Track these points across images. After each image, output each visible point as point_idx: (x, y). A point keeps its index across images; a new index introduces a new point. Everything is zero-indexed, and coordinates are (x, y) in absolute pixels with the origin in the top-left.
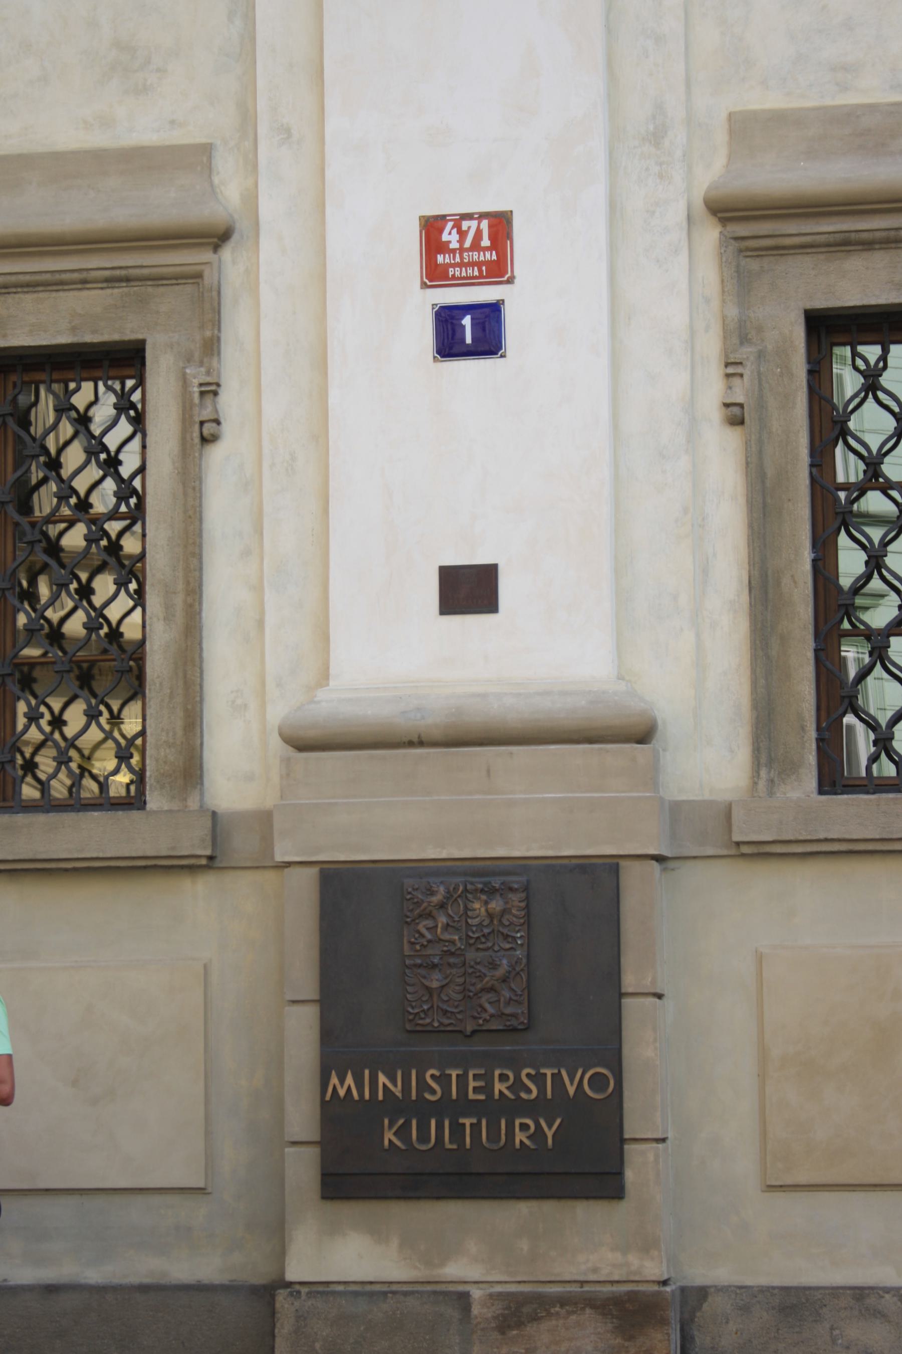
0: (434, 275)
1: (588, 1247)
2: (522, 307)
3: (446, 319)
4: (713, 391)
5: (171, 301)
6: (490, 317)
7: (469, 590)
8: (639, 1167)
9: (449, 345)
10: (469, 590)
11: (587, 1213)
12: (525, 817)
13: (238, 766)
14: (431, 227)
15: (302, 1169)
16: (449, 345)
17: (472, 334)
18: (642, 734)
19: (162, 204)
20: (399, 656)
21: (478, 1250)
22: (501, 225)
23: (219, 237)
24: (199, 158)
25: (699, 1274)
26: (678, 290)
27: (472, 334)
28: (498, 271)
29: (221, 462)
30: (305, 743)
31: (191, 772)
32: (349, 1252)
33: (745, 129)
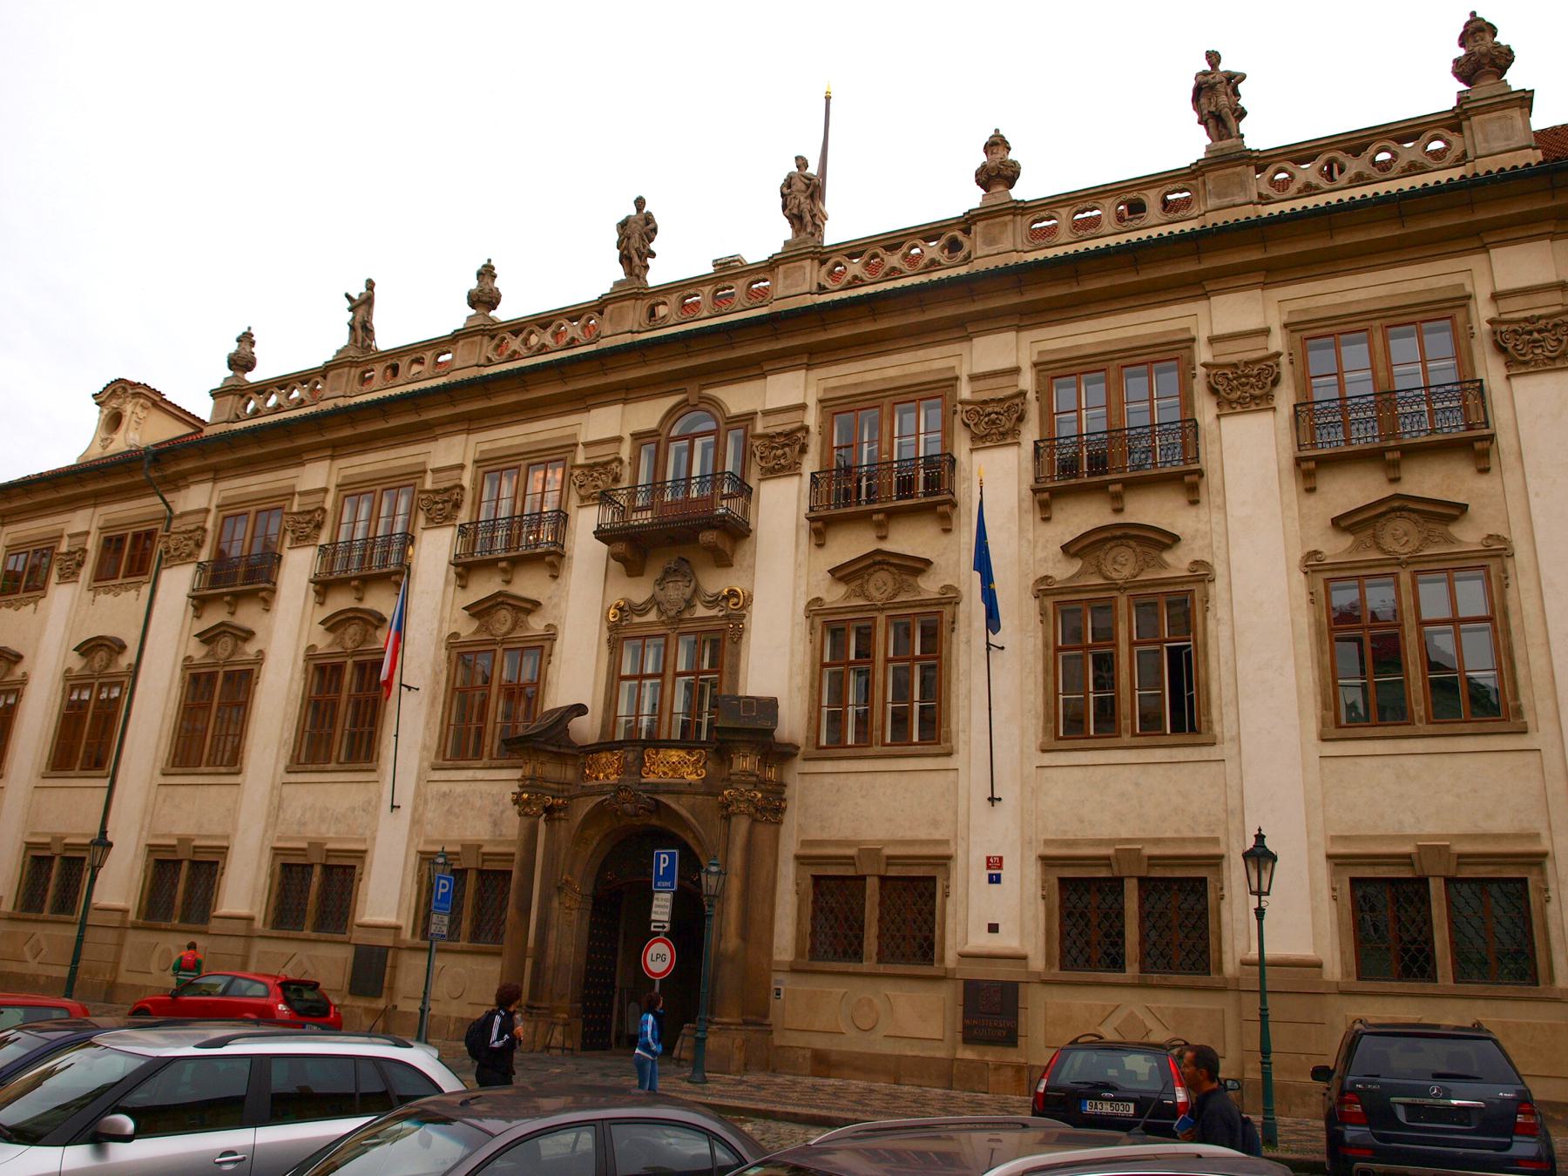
0: (989, 868)
1: (1012, 1056)
2: (1004, 874)
3: (990, 876)
4: (1040, 893)
5: (941, 869)
6: (998, 876)
7: (993, 928)
8: (1021, 1041)
9: (991, 881)
10: (993, 928)
11: (1011, 1050)
12: (1002, 972)
13: (951, 959)
14: (988, 858)
15: (959, 1037)
16: (991, 881)
17: (995, 879)
18: (1024, 958)
19: (940, 851)
20: (980, 941)
21: (991, 1055)
22: (1001, 859)
23: (949, 858)
24: (946, 842)
25: (1033, 1063)
26: (1034, 872)
27: (995, 879)
28: (1000, 867)
29: (949, 902)
30: (963, 956)
31: (942, 959)
32: (969, 1054)
33: (1047, 842)
